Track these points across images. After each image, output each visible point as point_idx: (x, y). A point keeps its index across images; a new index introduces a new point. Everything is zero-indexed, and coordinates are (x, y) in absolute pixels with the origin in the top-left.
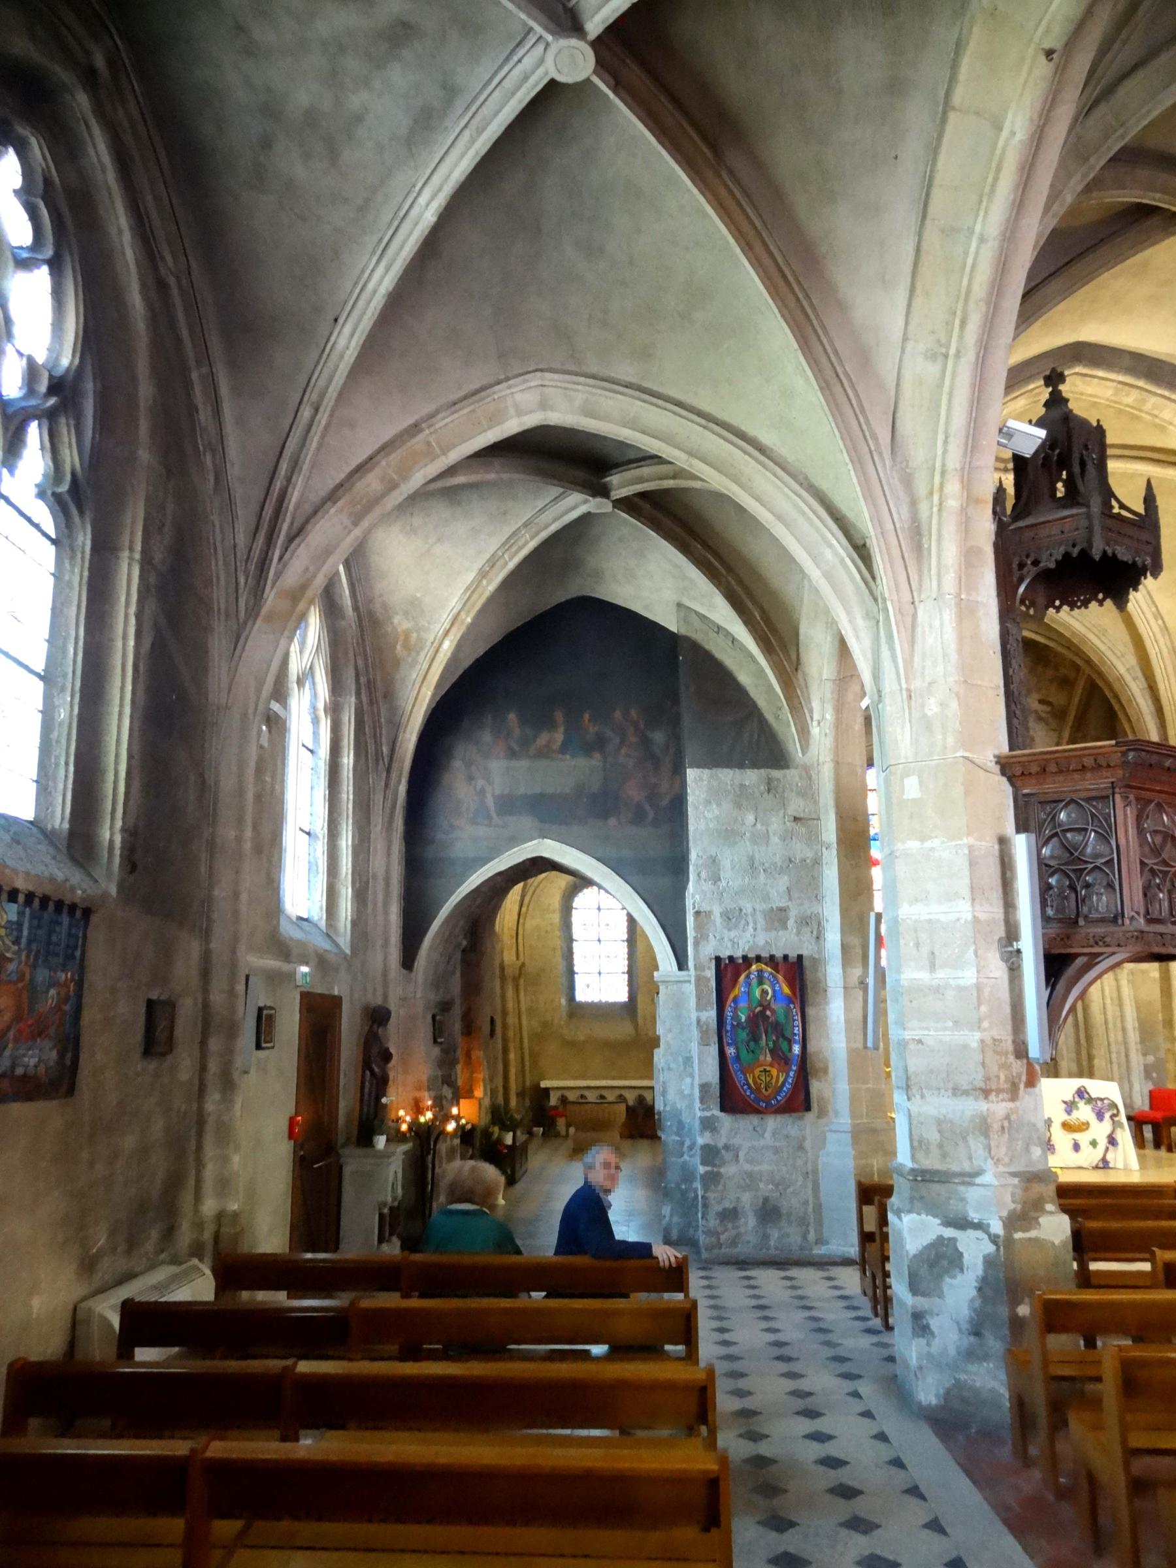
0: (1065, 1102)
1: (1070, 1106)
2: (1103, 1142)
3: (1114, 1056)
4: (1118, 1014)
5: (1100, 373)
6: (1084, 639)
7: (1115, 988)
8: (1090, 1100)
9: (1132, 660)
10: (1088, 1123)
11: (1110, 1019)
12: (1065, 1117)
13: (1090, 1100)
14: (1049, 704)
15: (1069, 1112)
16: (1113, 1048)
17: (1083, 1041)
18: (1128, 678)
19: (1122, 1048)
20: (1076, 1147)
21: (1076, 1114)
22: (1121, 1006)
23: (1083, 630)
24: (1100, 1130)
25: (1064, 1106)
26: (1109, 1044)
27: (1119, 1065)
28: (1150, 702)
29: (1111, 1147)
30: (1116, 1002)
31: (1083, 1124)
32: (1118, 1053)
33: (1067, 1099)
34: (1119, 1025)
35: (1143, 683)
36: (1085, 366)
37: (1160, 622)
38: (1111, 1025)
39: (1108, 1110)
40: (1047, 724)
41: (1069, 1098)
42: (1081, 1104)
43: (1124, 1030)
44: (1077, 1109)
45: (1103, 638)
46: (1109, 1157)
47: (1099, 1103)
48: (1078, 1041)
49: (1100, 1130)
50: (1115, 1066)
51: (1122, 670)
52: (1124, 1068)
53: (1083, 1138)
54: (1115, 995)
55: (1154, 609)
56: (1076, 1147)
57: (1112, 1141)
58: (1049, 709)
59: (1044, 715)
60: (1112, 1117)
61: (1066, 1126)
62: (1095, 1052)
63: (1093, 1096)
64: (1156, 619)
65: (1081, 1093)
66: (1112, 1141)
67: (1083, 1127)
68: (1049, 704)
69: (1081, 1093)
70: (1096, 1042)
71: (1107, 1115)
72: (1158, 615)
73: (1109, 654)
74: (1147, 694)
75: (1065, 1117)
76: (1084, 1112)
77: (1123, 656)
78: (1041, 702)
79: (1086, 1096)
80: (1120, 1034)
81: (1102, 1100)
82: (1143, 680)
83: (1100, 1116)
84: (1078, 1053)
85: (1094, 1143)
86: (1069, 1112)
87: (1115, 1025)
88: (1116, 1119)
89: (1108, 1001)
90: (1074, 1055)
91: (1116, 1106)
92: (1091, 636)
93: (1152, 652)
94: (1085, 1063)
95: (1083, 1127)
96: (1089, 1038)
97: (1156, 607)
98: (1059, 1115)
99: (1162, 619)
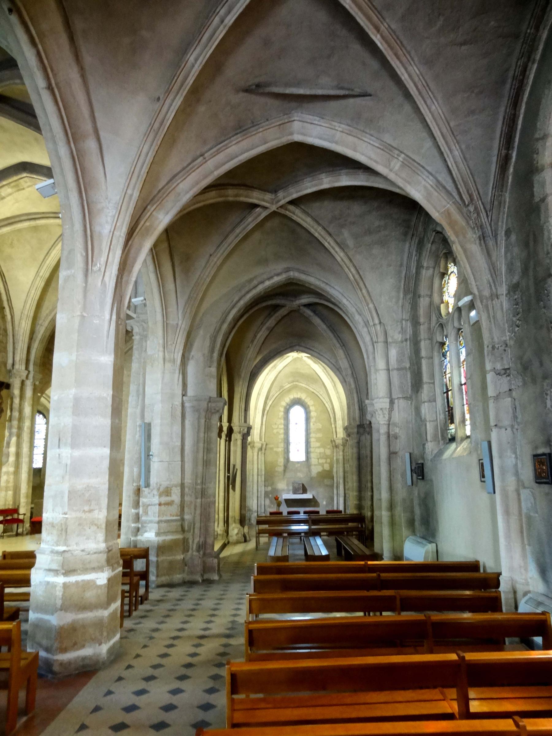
5: (35, 176)
36: (28, 173)
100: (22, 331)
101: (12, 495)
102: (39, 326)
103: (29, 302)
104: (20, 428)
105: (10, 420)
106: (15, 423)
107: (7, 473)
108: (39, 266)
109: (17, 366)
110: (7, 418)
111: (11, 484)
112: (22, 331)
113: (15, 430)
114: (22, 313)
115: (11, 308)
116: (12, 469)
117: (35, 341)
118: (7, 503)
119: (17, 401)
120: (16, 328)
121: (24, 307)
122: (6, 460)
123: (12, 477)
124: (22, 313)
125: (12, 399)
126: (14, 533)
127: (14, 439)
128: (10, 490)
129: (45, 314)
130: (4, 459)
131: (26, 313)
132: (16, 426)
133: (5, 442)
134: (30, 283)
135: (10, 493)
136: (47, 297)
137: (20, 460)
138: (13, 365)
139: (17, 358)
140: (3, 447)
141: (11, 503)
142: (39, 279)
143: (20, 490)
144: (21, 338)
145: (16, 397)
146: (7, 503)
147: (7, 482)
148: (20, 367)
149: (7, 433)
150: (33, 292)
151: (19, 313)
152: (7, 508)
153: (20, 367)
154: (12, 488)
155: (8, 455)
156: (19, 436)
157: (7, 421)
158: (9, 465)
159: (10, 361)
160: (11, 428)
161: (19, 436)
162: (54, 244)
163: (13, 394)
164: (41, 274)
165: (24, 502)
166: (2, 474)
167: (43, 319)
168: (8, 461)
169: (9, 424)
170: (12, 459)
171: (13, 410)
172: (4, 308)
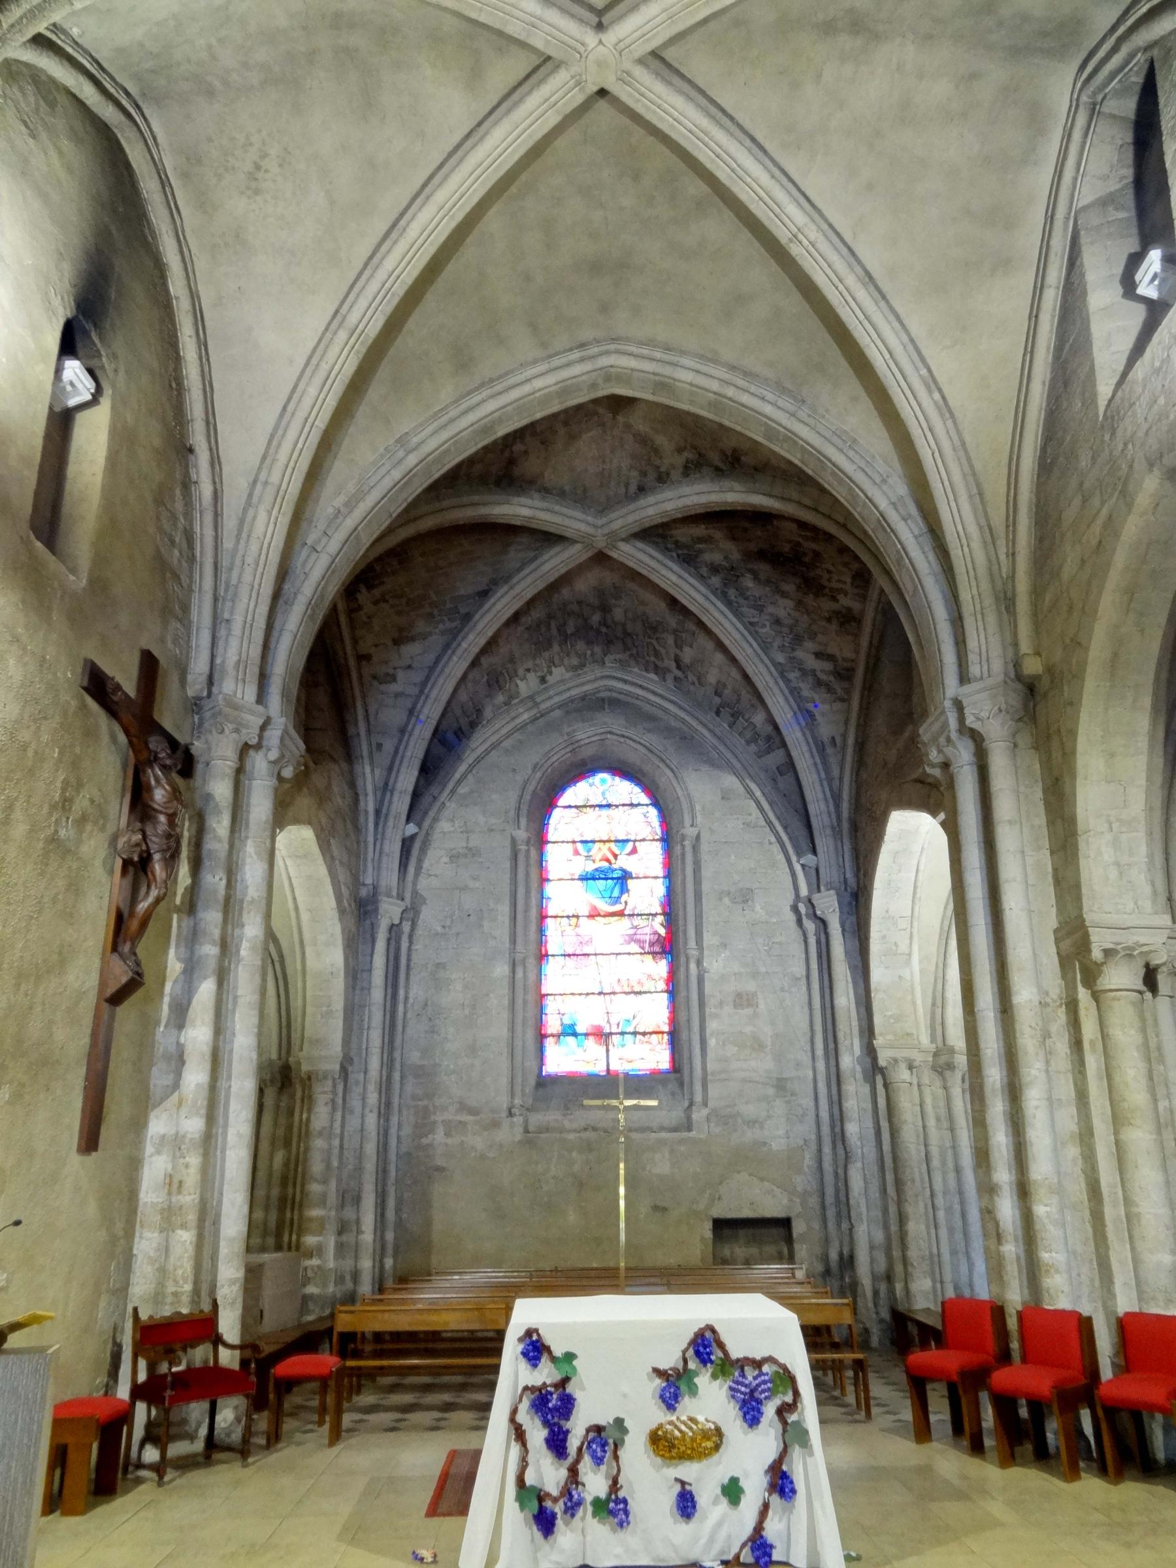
0: (658, 1372)
1: (673, 1385)
2: (755, 1487)
3: (941, 1214)
4: (948, 1144)
6: (821, 459)
7: (942, 1104)
8: (728, 1366)
9: (901, 489)
10: (719, 1432)
11: (934, 1151)
12: (657, 1416)
13: (728, 1366)
14: (831, 658)
15: (670, 1400)
16: (940, 1201)
17: (891, 1190)
18: (893, 517)
19: (956, 1199)
20: (686, 1504)
21: (688, 1407)
22: (952, 1129)
23: (817, 442)
24: (750, 1452)
25: (658, 1383)
26: (932, 1195)
27: (951, 1231)
28: (931, 556)
29: (775, 1500)
30: (945, 1124)
31: (706, 1435)
32: (949, 1210)
33: (665, 1364)
34: (950, 1164)
35: (919, 525)
37: (937, 396)
38: (936, 1163)
39: (773, 1393)
40: (830, 689)
41: (670, 1360)
42: (703, 1380)
43: (958, 1170)
44: (693, 1391)
45: (851, 453)
46: (773, 1529)
47: (750, 1373)
48: (884, 1191)
49: (750, 1452)
50: (943, 1233)
51: (883, 504)
52: (959, 1236)
53: (705, 1477)
54: (943, 1112)
55: (924, 372)
56: (686, 1504)
57: (780, 1482)
58: (828, 666)
59: (823, 677)
60: (782, 1411)
61: (663, 1444)
62: (909, 1209)
63: (736, 1351)
64: (930, 392)
65: (705, 1345)
66: (780, 1482)
67: (710, 1441)
68: (831, 658)
69: (705, 1345)
70: (909, 1191)
71: (769, 1410)
72: (932, 383)
73: (859, 477)
74: (927, 541)
75: (657, 1416)
76: (711, 1401)
77: (884, 481)
78: (818, 655)
79: (717, 1355)
80: (952, 1176)
81: (757, 1364)
82: (919, 520)
83: (751, 1413)
84: (885, 1211)
85: (732, 1491)
86: (670, 1400)
87: (944, 1163)
88: (792, 1418)
89: (931, 1122)
90: (877, 1213)
91: (787, 1378)
92: (830, 451)
93: (926, 454)
94: (894, 1228)
95: (710, 1441)
96: (899, 1183)
97: (929, 370)
98: (644, 1413)
99: (940, 390)
100: (254, 547)
101: (191, 1250)
102: (305, 552)
103: (292, 434)
104: (226, 946)
105: (191, 906)
106: (211, 918)
107: (175, 1143)
108: (345, 289)
109: (227, 686)
110: (178, 900)
111: (189, 1198)
112: (254, 547)
113: (209, 950)
114: (255, 482)
115: (215, 461)
116: (194, 1125)
117: (289, 603)
118: (171, 1288)
119: (220, 826)
120: (228, 544)
121: (264, 458)
122: (168, 1080)
123: (194, 1160)
124: (255, 482)
125: (200, 820)
126: (199, 1446)
127: (206, 989)
128: (184, 1226)
129: (330, 510)
130: (159, 1078)
131: (275, 478)
132: (217, 933)
133: (166, 1000)
134: (300, 361)
135: (185, 1238)
136: (346, 442)
137: (222, 1084)
138: (210, 681)
139: (231, 654)
140: (158, 1023)
141: (188, 1287)
142: (342, 335)
143: (216, 1223)
144: (247, 577)
145: (219, 812)
146: (171, 1288)
147: (172, 1184)
148: (238, 689)
149: (174, 965)
150: (312, 391)
151: (243, 484)
152: (166, 1311)
153: (238, 689)
154: (192, 1217)
155: (179, 1060)
156: (222, 977)
157: (178, 910)
158: (180, 1104)
159: (199, 666)
160: (193, 937)
161: (222, 977)
162: (425, 185)
163: (208, 797)
164: (354, 318)
165: (232, 1282)
166: (149, 1149)
167: (321, 526)
168: (176, 1085)
169: (187, 923)
170: (195, 1077)
171: (207, 863)
172: (191, 450)
